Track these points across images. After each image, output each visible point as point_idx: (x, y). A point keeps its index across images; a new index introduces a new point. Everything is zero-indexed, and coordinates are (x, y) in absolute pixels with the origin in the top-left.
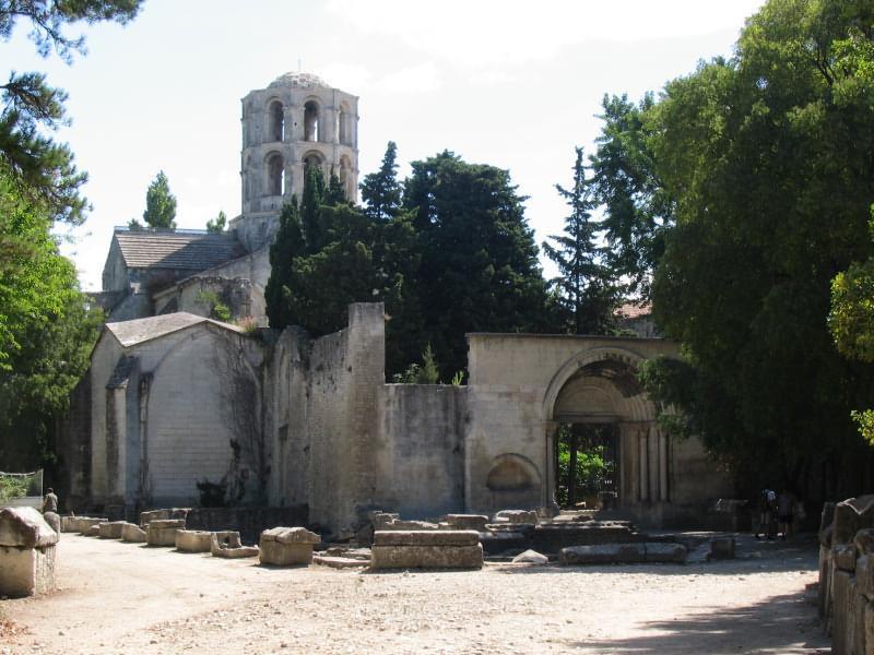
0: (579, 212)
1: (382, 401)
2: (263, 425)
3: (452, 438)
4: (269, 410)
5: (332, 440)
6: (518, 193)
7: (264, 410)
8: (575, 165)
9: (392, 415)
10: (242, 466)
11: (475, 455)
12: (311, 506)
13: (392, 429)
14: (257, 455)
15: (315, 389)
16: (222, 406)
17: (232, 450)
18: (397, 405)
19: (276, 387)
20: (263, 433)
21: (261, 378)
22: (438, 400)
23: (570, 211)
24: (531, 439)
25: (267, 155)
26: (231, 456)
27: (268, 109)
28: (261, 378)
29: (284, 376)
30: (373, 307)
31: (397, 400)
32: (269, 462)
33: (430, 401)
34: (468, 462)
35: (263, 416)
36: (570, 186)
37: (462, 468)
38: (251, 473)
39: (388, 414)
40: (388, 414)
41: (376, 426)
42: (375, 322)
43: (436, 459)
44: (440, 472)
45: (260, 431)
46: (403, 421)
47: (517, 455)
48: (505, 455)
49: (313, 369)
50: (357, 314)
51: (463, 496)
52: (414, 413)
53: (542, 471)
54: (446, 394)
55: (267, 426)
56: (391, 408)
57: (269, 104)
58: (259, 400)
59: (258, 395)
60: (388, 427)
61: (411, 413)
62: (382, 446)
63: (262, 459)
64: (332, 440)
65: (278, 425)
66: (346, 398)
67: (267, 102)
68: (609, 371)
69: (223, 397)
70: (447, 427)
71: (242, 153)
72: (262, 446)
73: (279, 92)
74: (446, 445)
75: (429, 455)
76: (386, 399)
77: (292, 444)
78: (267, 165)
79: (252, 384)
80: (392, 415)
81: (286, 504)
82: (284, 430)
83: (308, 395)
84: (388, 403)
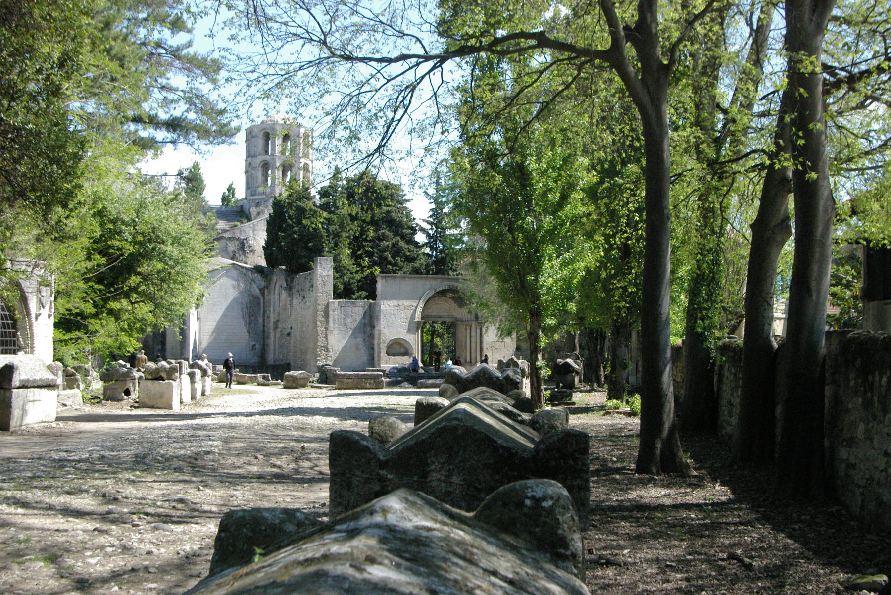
15: (294, 301)
21: (263, 295)
23: (433, 206)
28: (263, 295)
61: (346, 316)
74: (364, 332)
79: (258, 298)
81: (278, 363)
82: (276, 323)
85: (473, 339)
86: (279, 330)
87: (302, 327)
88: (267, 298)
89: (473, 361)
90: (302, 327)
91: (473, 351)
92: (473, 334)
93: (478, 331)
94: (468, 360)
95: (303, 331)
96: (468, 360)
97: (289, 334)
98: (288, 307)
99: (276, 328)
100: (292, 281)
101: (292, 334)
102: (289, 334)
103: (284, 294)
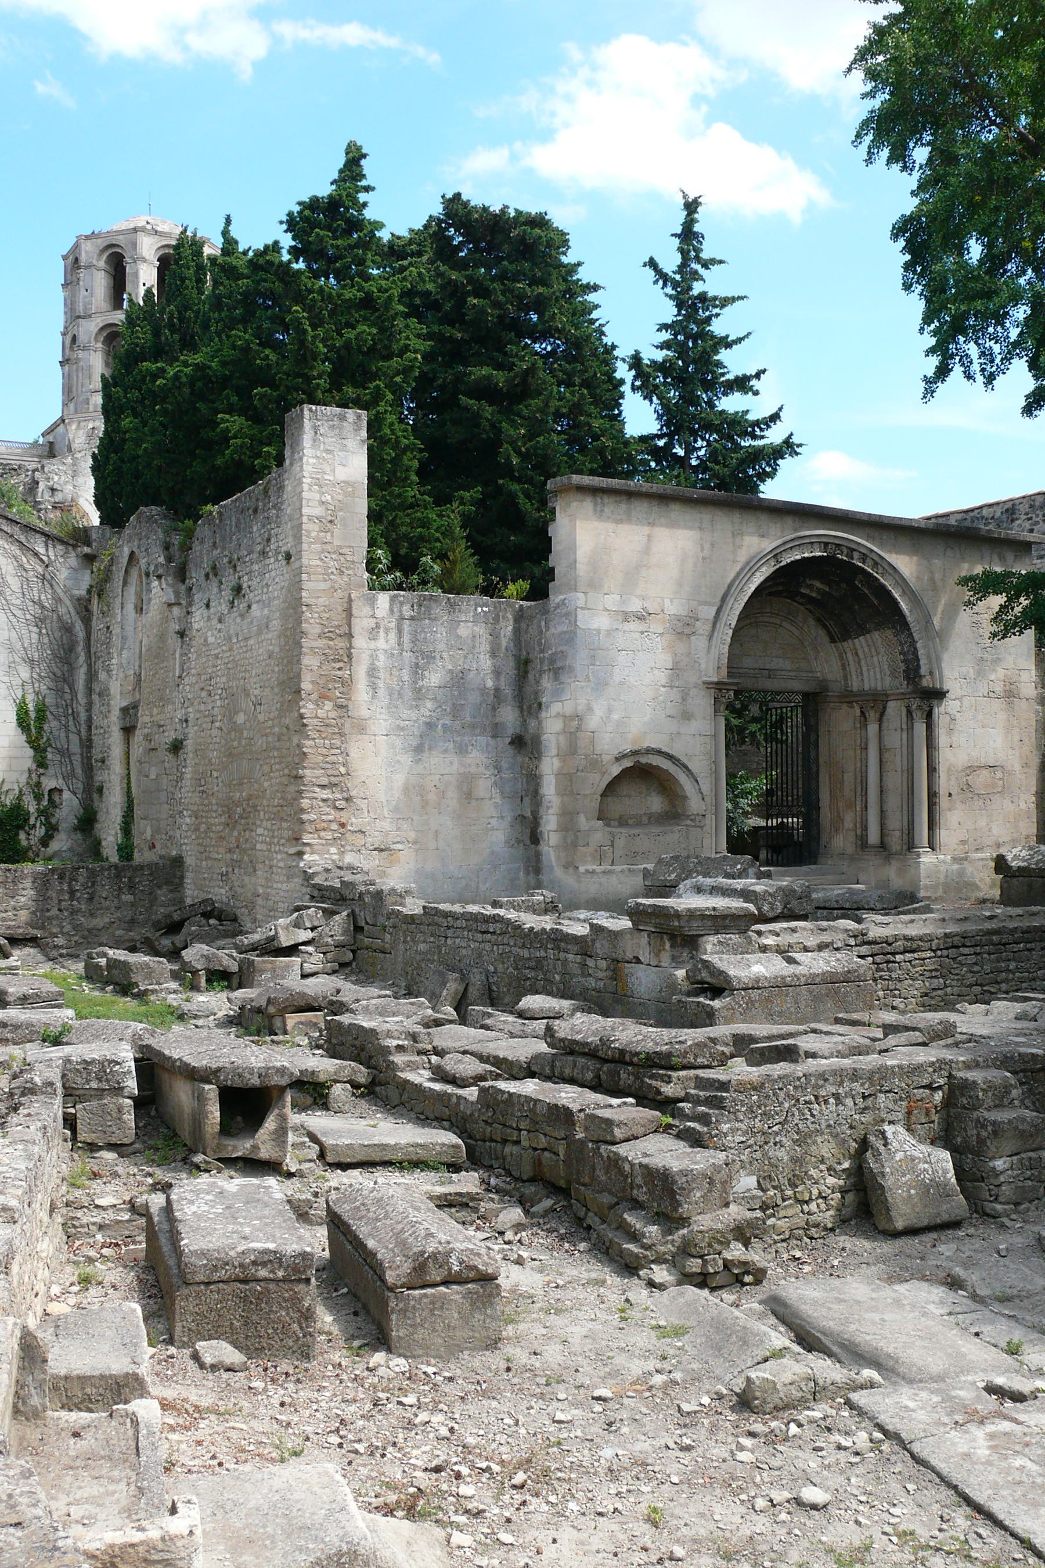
0: (688, 318)
1: (362, 623)
2: (89, 706)
3: (509, 715)
4: (102, 676)
5: (241, 718)
6: (584, 276)
7: (92, 676)
8: (679, 230)
9: (382, 661)
10: (49, 783)
11: (571, 750)
12: (190, 861)
13: (382, 692)
14: (77, 760)
15: (198, 619)
16: (11, 667)
17: (30, 752)
18: (393, 636)
19: (116, 630)
20: (89, 720)
21: (87, 621)
22: (481, 630)
23: (669, 312)
24: (686, 716)
25: (102, 329)
26: (29, 763)
27: (102, 264)
28: (87, 621)
29: (130, 607)
30: (342, 418)
31: (393, 625)
32: (99, 777)
33: (464, 631)
34: (550, 767)
35: (89, 691)
36: (670, 262)
37: (532, 782)
38: (66, 795)
39: (373, 657)
40: (373, 657)
41: (347, 684)
42: (344, 448)
43: (477, 759)
44: (484, 787)
45: (83, 716)
46: (406, 676)
47: (659, 752)
48: (635, 753)
49: (196, 575)
50: (307, 424)
51: (535, 838)
52: (430, 657)
53: (706, 787)
54: (496, 620)
55: (96, 709)
56: (381, 643)
57: (105, 257)
58: (82, 659)
59: (80, 648)
60: (374, 687)
62: (361, 728)
63: (89, 770)
64: (241, 718)
65: (118, 701)
66: (276, 624)
67: (103, 251)
68: (817, 584)
69: (11, 650)
70: (497, 690)
71: (64, 334)
72: (88, 744)
73: (121, 240)
74: (496, 730)
75: (462, 750)
76: (372, 623)
77: (148, 738)
78: (100, 345)
80: (382, 661)
82: (129, 712)
83: (182, 634)
84: (373, 633)
85: (897, 761)
86: (138, 737)
87: (231, 712)
88: (98, 625)
89: (895, 842)
90: (231, 712)
91: (893, 802)
92: (895, 739)
93: (920, 728)
94: (873, 837)
95: (235, 728)
96: (873, 837)
97: (176, 747)
98: (173, 641)
99: (128, 731)
100: (186, 548)
101: (189, 744)
102: (176, 747)
103: (160, 592)
